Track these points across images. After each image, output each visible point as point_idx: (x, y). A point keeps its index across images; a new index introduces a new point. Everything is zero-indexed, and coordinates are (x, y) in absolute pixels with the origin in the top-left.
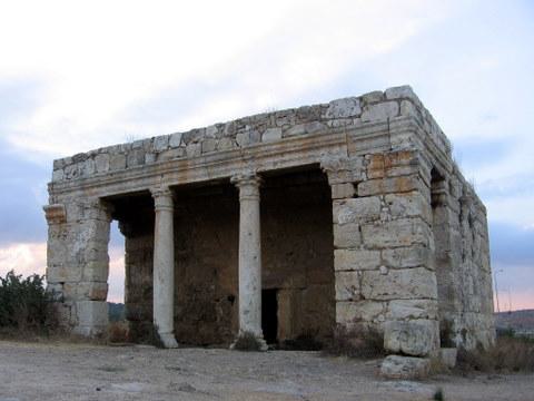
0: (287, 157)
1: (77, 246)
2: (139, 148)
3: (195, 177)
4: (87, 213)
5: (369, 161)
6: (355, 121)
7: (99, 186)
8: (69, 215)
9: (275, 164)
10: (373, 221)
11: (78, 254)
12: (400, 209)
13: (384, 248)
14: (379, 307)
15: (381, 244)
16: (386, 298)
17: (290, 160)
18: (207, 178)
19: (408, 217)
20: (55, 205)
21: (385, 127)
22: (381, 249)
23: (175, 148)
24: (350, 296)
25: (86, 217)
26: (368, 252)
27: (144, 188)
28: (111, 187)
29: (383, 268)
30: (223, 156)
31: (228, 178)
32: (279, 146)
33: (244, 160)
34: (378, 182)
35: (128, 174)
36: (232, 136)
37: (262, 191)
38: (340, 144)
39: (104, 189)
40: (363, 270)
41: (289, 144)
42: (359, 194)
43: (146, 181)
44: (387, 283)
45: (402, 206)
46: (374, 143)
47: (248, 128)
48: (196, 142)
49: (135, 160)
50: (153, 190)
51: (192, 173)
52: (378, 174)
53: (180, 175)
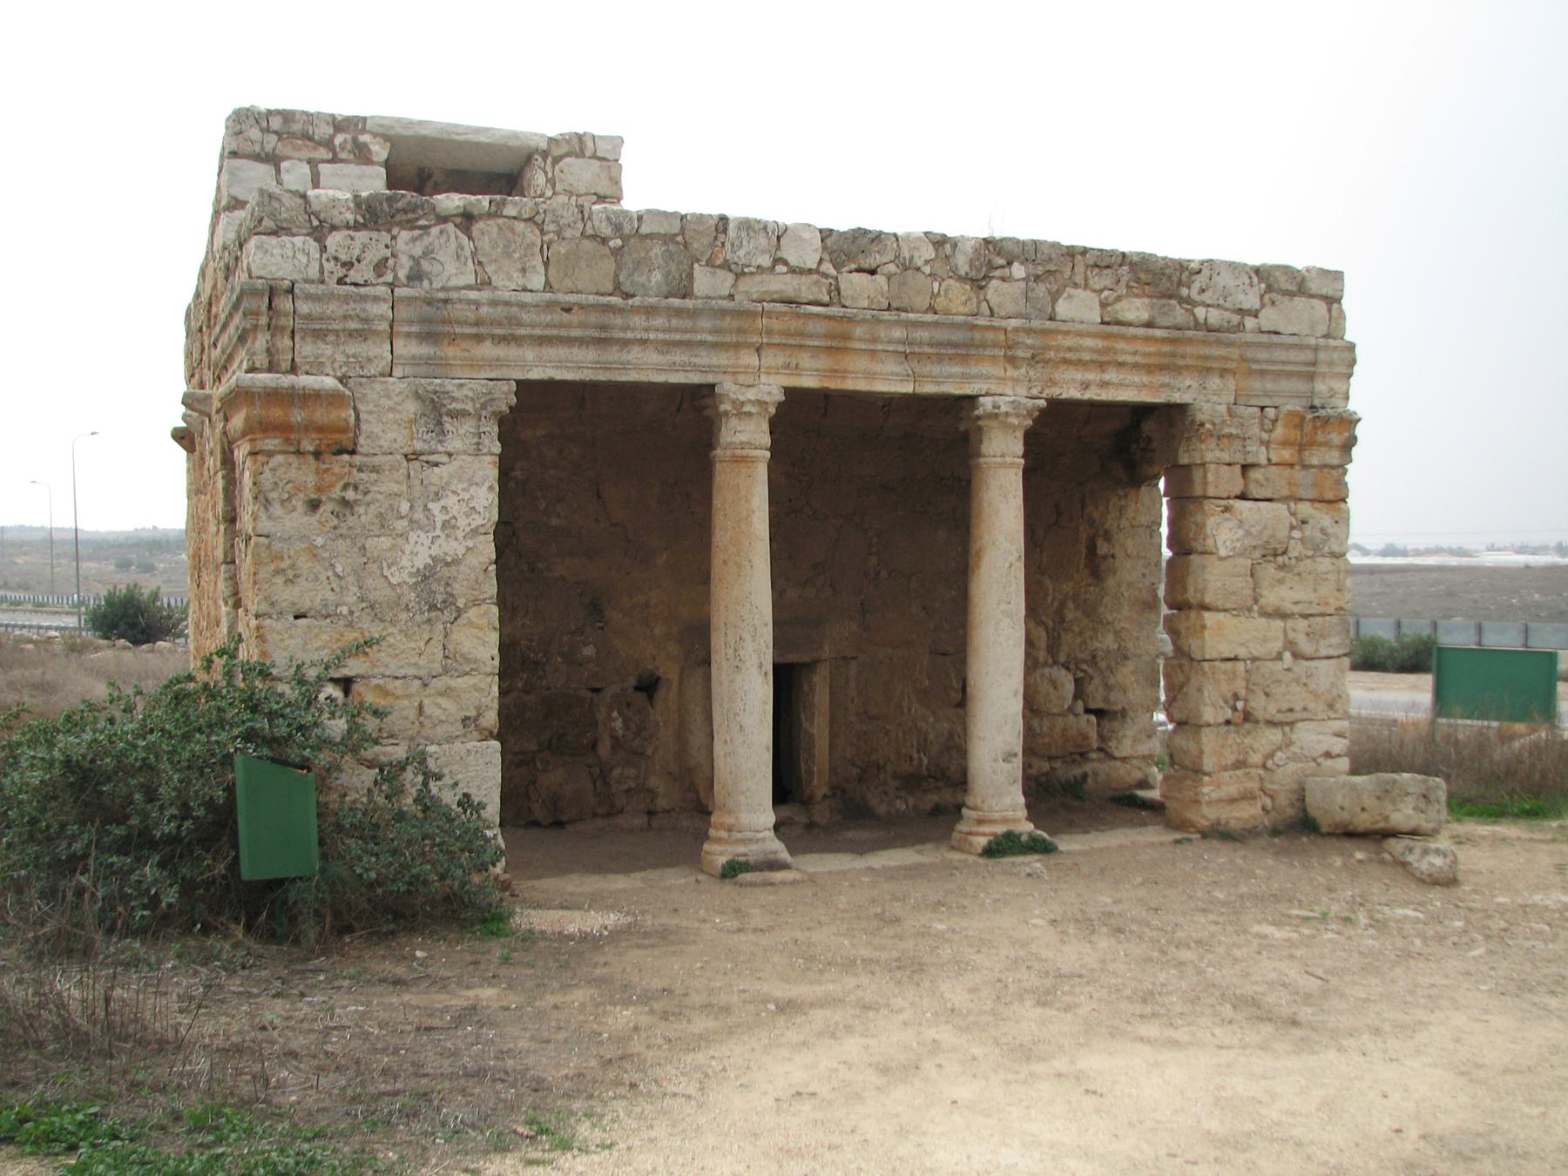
0: (1111, 375)
1: (419, 551)
2: (668, 239)
3: (871, 376)
4: (459, 436)
5: (1274, 422)
6: (1250, 323)
8: (370, 426)
9: (1086, 386)
10: (1276, 555)
11: (425, 576)
14: (1275, 736)
15: (1288, 607)
16: (1290, 717)
17: (1121, 385)
18: (908, 388)
20: (286, 380)
22: (1283, 616)
24: (1229, 714)
25: (454, 444)
26: (1263, 620)
27: (695, 378)
28: (561, 352)
29: (1287, 655)
30: (958, 336)
31: (972, 399)
32: (1100, 343)
33: (1012, 361)
34: (1287, 471)
35: (638, 320)
36: (978, 284)
38: (1223, 372)
39: (530, 354)
40: (1254, 659)
41: (1121, 345)
42: (1255, 492)
43: (704, 358)
44: (1295, 688)
45: (1323, 531)
46: (1285, 385)
47: (1018, 270)
48: (873, 272)
49: (657, 277)
51: (862, 363)
52: (1287, 454)
53: (824, 362)
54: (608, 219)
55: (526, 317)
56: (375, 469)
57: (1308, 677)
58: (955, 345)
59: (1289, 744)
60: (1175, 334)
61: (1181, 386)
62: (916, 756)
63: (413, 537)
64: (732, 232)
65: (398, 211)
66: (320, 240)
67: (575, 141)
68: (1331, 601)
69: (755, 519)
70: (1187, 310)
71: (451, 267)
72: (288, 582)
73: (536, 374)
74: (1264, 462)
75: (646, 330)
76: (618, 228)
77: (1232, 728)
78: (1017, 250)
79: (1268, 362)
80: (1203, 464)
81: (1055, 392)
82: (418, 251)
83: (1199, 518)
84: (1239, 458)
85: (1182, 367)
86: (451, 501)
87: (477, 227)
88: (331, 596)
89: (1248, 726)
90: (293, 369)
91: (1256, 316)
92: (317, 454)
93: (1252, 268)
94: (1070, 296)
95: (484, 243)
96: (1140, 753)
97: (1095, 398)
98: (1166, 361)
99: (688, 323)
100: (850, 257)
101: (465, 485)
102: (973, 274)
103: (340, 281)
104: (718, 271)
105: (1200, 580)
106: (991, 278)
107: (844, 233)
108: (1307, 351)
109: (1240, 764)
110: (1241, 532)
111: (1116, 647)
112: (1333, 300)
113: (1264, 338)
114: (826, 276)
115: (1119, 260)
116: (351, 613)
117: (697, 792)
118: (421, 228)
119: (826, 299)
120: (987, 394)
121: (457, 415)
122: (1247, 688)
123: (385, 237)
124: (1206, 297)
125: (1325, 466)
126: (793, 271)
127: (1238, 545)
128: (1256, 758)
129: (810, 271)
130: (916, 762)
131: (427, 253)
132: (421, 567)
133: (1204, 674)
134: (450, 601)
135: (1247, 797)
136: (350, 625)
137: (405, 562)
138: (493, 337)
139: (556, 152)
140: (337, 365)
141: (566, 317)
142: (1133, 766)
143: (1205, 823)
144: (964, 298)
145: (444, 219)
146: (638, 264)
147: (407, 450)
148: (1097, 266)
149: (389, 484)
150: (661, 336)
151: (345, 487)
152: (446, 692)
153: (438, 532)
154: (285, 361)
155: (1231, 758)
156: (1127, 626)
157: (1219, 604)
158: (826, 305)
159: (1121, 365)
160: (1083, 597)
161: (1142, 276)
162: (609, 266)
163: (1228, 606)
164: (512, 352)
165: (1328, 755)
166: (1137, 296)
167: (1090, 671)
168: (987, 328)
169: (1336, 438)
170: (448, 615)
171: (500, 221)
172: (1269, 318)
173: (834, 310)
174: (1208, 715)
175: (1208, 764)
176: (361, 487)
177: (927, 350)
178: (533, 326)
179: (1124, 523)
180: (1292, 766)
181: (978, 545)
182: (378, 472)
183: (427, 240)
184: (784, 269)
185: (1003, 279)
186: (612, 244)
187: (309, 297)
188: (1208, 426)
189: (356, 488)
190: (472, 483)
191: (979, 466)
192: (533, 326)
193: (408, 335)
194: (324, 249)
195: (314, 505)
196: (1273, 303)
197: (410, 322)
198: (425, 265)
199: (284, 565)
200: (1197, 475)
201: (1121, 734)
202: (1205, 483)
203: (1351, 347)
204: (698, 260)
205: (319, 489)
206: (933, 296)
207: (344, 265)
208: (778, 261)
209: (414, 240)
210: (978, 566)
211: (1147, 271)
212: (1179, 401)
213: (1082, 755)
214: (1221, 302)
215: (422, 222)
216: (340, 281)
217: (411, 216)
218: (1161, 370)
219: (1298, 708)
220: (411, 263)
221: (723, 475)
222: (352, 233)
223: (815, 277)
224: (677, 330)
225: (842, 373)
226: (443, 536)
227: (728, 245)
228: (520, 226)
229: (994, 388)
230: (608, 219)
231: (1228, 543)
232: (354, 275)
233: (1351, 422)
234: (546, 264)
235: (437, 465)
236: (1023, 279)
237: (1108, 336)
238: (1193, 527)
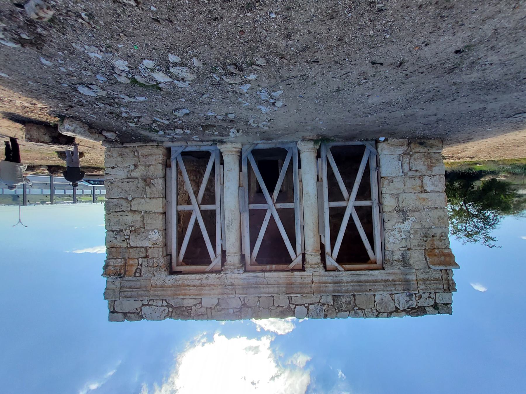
0: (198, 283)
1: (407, 225)
5: (136, 272)
7: (387, 281)
11: (405, 219)
12: (118, 237)
13: (128, 212)
14: (134, 174)
15: (130, 214)
17: (194, 280)
19: (113, 231)
21: (122, 294)
23: (301, 305)
28: (370, 278)
33: (233, 284)
35: (350, 288)
37: (291, 259)
39: (379, 277)
40: (143, 198)
44: (127, 189)
45: (116, 238)
47: (231, 311)
53: (293, 280)
54: (358, 315)
55: (382, 287)
56: (419, 245)
57: (122, 192)
59: (128, 172)
61: (172, 281)
63: (409, 229)
65: (416, 312)
66: (435, 302)
70: (169, 304)
72: (440, 217)
75: (347, 286)
76: (356, 313)
79: (139, 291)
82: (411, 302)
85: (172, 287)
86: (400, 238)
88: (429, 213)
89: (145, 178)
93: (145, 319)
95: (392, 305)
98: (178, 288)
99: (336, 288)
102: (247, 309)
103: (430, 293)
112: (113, 312)
114: (293, 304)
116: (424, 209)
121: (398, 261)
122: (145, 189)
123: (419, 305)
124: (162, 308)
125: (115, 259)
127: (150, 233)
129: (298, 305)
131: (408, 302)
137: (411, 222)
143: (161, 148)
146: (349, 303)
147: (411, 251)
148: (203, 315)
149: (415, 242)
151: (426, 241)
152: (398, 189)
154: (444, 272)
157: (157, 215)
159: (194, 286)
164: (385, 277)
165: (113, 168)
166: (189, 307)
169: (111, 268)
172: (138, 304)
173: (290, 295)
183: (408, 305)
184: (306, 305)
186: (357, 308)
187: (440, 289)
188: (163, 270)
190: (394, 243)
192: (379, 285)
193: (413, 280)
194: (435, 300)
195: (433, 236)
196: (136, 309)
197: (413, 284)
203: (105, 298)
204: (332, 305)
205: (434, 240)
209: (412, 305)
212: (173, 276)
214: (157, 308)
229: (239, 276)
230: (358, 315)
231: (154, 233)
232: (427, 295)
233: (105, 274)
234: (375, 301)
235: (403, 247)
237: (200, 295)
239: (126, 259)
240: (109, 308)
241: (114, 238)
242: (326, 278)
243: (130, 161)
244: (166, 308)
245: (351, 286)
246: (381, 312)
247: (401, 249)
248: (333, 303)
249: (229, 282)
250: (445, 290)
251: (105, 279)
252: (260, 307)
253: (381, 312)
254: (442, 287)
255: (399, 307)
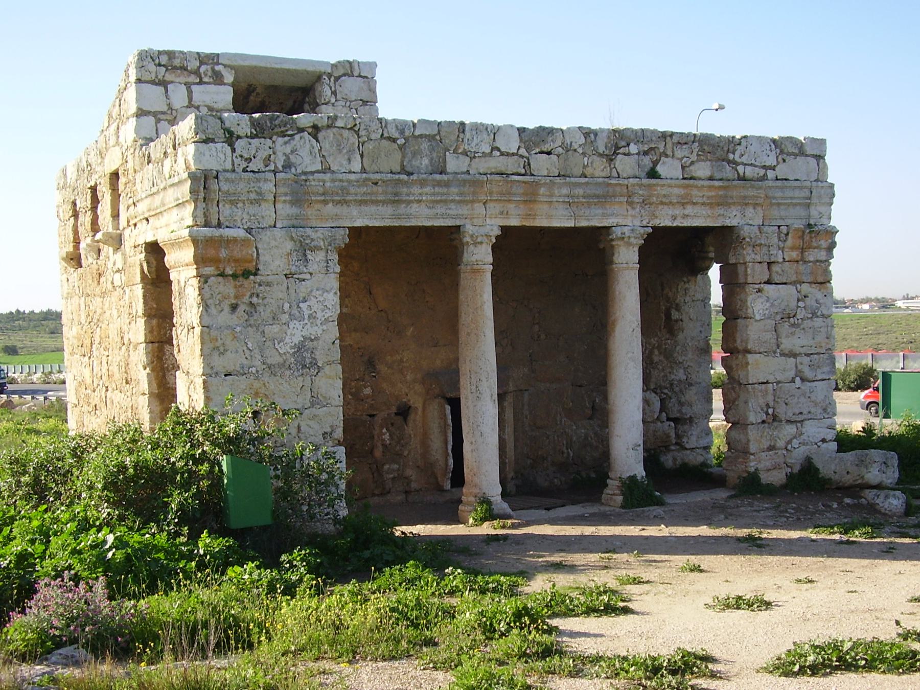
0: (689, 210)
1: (296, 333)
2: (431, 138)
5: (787, 234)
6: (771, 174)
9: (674, 218)
10: (789, 318)
11: (300, 348)
14: (791, 430)
15: (798, 350)
16: (800, 418)
18: (570, 224)
19: (823, 316)
20: (216, 232)
22: (794, 355)
23: (508, 154)
25: (313, 267)
28: (373, 209)
29: (798, 379)
30: (599, 191)
35: (416, 190)
36: (610, 160)
38: (755, 206)
39: (354, 211)
40: (778, 382)
42: (777, 279)
43: (454, 210)
44: (802, 399)
45: (817, 301)
47: (633, 148)
48: (549, 153)
49: (426, 161)
50: (469, 229)
52: (794, 255)
54: (397, 126)
56: (269, 284)
58: (598, 197)
59: (802, 434)
60: (726, 183)
61: (731, 215)
62: (566, 451)
64: (468, 135)
66: (231, 145)
67: (348, 65)
68: (823, 345)
69: (485, 307)
70: (733, 168)
71: (307, 160)
73: (358, 223)
74: (781, 260)
76: (402, 132)
77: (766, 425)
78: (633, 137)
79: (782, 198)
80: (745, 263)
81: (657, 222)
82: (288, 150)
83: (743, 296)
84: (766, 259)
85: (730, 204)
86: (312, 302)
87: (320, 136)
88: (245, 362)
89: (775, 424)
90: (219, 225)
91: (774, 170)
92: (235, 276)
94: (664, 163)
96: (702, 446)
97: (680, 225)
99: (445, 190)
100: (536, 145)
101: (320, 292)
102: (607, 152)
103: (245, 170)
104: (460, 156)
105: (745, 335)
106: (618, 154)
107: (533, 130)
108: (805, 190)
109: (771, 448)
110: (768, 304)
111: (685, 378)
112: (820, 158)
113: (779, 183)
114: (522, 156)
115: (692, 139)
116: (257, 371)
117: (436, 478)
118: (289, 136)
119: (523, 171)
120: (617, 226)
123: (269, 142)
124: (744, 159)
125: (817, 261)
126: (502, 154)
127: (767, 312)
128: (781, 443)
129: (513, 154)
130: (565, 455)
132: (297, 343)
133: (748, 392)
134: (314, 363)
135: (776, 467)
136: (257, 379)
137: (287, 340)
138: (333, 201)
139: (336, 74)
140: (244, 221)
141: (375, 188)
142: (698, 454)
144: (602, 167)
145: (301, 130)
146: (414, 154)
150: (429, 198)
153: (306, 321)
155: (766, 444)
156: (691, 364)
158: (523, 175)
160: (664, 347)
161: (706, 147)
162: (398, 156)
163: (762, 350)
165: (824, 441)
166: (703, 160)
167: (670, 394)
168: (616, 185)
169: (824, 244)
170: (313, 371)
171: (335, 130)
172: (781, 171)
174: (752, 418)
175: (753, 448)
176: (261, 295)
177: (581, 200)
178: (356, 195)
179: (687, 299)
180: (803, 448)
181: (612, 318)
182: (270, 286)
183: (293, 143)
184: (498, 153)
185: (625, 154)
186: (398, 142)
188: (748, 240)
189: (258, 296)
191: (612, 270)
193: (285, 201)
194: (234, 150)
195: (234, 307)
196: (784, 161)
197: (286, 195)
198: (293, 158)
199: (218, 344)
200: (741, 269)
201: (690, 433)
202: (746, 275)
204: (449, 150)
205: (236, 297)
206: (585, 167)
207: (246, 160)
208: (493, 149)
209: (286, 143)
210: (614, 331)
211: (709, 145)
213: (666, 447)
214: (753, 162)
215: (290, 132)
216: (245, 170)
217: (283, 129)
218: (719, 205)
219: (805, 412)
220: (284, 157)
221: (465, 279)
222: (249, 140)
223: (516, 157)
224: (438, 194)
225: (533, 216)
226: (309, 324)
227: (466, 140)
228: (346, 133)
229: (621, 222)
231: (761, 311)
233: (833, 233)
234: (362, 156)
236: (637, 154)
237: (687, 187)
238: (739, 302)
239: (801, 260)
240: (825, 165)
241: (821, 301)
242: (460, 212)
243: (798, 455)
244: (739, 160)
245: (413, 195)
246: (349, 129)
247: (308, 276)
248: (445, 155)
249: (638, 210)
250: (217, 177)
251: (832, 223)
252: (582, 153)
253: (349, 129)
254: (221, 184)
255: (311, 137)
